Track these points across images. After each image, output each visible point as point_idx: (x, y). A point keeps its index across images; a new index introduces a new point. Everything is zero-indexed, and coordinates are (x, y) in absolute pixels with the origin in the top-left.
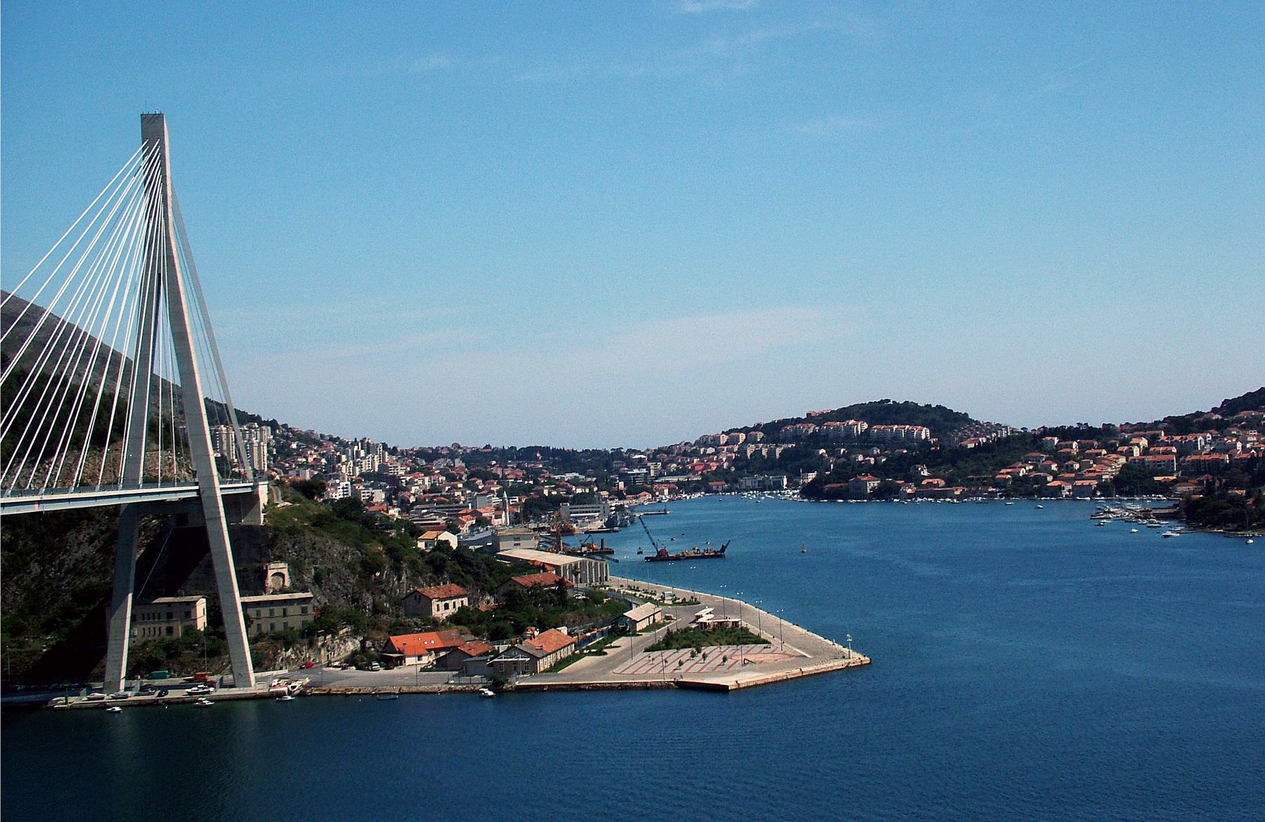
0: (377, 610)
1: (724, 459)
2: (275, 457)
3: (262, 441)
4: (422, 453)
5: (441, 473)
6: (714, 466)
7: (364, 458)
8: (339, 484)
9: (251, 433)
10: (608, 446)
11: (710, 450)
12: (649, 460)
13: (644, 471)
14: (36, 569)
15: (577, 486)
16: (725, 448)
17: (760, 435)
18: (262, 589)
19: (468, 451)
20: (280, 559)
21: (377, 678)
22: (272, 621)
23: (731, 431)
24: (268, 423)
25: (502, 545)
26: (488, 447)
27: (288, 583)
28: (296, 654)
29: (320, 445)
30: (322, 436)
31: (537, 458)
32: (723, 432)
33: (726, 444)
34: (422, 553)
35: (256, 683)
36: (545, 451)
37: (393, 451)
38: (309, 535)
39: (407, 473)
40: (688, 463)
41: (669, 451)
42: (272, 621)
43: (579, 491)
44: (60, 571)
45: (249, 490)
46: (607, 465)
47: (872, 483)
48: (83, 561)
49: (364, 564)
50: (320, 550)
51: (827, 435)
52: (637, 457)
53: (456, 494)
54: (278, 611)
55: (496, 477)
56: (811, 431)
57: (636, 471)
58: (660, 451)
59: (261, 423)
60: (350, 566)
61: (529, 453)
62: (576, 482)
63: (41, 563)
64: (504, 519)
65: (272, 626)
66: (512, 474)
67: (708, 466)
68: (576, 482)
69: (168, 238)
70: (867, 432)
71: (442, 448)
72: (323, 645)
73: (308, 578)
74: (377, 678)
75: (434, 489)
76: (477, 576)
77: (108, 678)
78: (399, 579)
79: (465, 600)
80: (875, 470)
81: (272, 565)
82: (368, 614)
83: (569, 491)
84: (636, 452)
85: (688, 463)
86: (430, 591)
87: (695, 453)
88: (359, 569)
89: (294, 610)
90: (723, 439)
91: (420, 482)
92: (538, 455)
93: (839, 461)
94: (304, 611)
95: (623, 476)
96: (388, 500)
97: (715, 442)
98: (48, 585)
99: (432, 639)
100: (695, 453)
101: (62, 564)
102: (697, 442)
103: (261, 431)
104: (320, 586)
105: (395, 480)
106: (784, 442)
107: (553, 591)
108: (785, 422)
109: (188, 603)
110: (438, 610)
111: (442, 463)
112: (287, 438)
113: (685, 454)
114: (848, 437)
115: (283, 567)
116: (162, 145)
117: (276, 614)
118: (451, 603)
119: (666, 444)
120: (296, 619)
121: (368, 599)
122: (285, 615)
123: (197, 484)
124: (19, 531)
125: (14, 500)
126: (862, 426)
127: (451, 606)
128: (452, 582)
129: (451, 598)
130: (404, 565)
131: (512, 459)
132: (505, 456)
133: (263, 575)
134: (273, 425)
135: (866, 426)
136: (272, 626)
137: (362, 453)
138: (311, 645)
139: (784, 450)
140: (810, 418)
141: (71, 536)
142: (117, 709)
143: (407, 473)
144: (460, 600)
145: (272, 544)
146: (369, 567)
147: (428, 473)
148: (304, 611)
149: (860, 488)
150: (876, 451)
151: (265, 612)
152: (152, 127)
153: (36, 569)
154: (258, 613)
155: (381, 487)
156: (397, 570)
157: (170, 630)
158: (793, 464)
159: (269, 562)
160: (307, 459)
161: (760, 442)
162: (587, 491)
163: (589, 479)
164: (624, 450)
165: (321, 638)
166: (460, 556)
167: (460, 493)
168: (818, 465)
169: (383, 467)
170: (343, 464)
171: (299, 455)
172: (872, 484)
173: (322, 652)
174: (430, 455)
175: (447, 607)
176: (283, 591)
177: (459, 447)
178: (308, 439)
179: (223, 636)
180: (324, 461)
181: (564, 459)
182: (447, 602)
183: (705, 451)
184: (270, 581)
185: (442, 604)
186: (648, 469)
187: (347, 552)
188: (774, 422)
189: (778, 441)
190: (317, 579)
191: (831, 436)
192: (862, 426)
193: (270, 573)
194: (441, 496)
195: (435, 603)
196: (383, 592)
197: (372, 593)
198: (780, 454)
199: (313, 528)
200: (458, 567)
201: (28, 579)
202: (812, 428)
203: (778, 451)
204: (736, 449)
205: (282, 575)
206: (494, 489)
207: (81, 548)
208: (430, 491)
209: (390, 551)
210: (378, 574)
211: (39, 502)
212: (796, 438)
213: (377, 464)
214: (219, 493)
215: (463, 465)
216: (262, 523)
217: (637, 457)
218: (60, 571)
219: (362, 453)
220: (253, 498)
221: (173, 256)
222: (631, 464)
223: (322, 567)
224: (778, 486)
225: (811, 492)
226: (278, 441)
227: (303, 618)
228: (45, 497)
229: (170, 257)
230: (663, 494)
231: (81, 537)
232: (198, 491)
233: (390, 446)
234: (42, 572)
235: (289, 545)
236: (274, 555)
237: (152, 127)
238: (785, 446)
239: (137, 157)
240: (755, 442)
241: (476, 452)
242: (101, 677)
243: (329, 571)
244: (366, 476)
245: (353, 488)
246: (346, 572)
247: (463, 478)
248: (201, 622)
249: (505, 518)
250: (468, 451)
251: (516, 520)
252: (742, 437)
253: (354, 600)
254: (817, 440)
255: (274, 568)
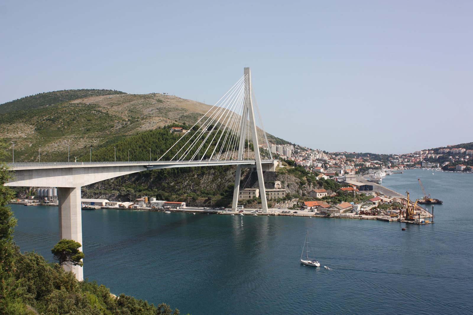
0: (304, 195)
1: (421, 158)
2: (293, 154)
3: (289, 150)
4: (334, 154)
5: (339, 159)
6: (418, 160)
7: (317, 155)
8: (309, 162)
9: (287, 147)
10: (388, 153)
11: (418, 156)
12: (399, 158)
13: (398, 161)
14: (220, 180)
15: (376, 164)
16: (422, 155)
17: (432, 152)
18: (273, 187)
19: (349, 154)
20: (279, 180)
21: (300, 213)
22: (275, 196)
23: (424, 150)
24: (293, 145)
25: (347, 179)
26: (354, 153)
27: (280, 187)
28: (280, 204)
29: (307, 151)
30: (308, 148)
31: (368, 156)
32: (422, 151)
33: (423, 154)
34: (317, 181)
35: (269, 211)
36: (370, 154)
37: (327, 153)
38: (287, 175)
39: (329, 159)
40: (411, 159)
41: (405, 156)
42: (275, 196)
43: (377, 166)
44: (225, 181)
45: (272, 162)
46: (387, 159)
47: (463, 167)
48: (231, 178)
49: (300, 182)
50: (289, 179)
51: (453, 153)
52: (396, 157)
53: (342, 165)
54: (276, 193)
55: (353, 161)
56: (448, 151)
57: (395, 161)
58: (403, 155)
59: (290, 144)
60: (297, 183)
61: (365, 155)
62: (377, 163)
63: (221, 179)
64: (353, 173)
65: (275, 197)
66: (359, 161)
67: (416, 160)
68: (377, 163)
69: (250, 98)
70: (465, 152)
71: (342, 153)
72: (287, 203)
73: (286, 185)
74: (300, 213)
75: (336, 164)
76: (331, 188)
77: (233, 207)
78: (310, 187)
79: (326, 193)
80: (464, 163)
81: (276, 182)
82: (301, 195)
83: (374, 166)
84: (396, 155)
85: (411, 159)
86: (316, 190)
87: (413, 156)
88: (299, 184)
89: (280, 193)
90: (422, 152)
91: (332, 162)
92: (368, 155)
93: (456, 160)
94: (283, 194)
95: (391, 162)
96: (322, 166)
97: (419, 154)
98: (222, 184)
99: (316, 203)
100: (413, 156)
101: (226, 179)
102: (414, 153)
103: (290, 146)
104: (289, 188)
105: (325, 161)
106: (440, 154)
107: (351, 192)
108: (440, 148)
109: (254, 190)
110: (318, 195)
111: (339, 157)
112: (298, 149)
113: (410, 156)
114: (459, 154)
115: (279, 182)
116: (249, 75)
117: (276, 194)
118: (322, 194)
119: (405, 153)
120: (281, 197)
121: (301, 192)
122: (278, 194)
123: (255, 160)
124: (216, 170)
125: (201, 163)
126: (463, 150)
127: (322, 195)
128: (324, 189)
129: (322, 193)
130: (312, 183)
131: (361, 156)
132: (358, 155)
133: (274, 184)
134: (294, 145)
135: (465, 150)
136: (275, 197)
137: (317, 153)
138: (284, 202)
139: (440, 156)
140: (448, 147)
141: (228, 172)
142: (234, 215)
143: (329, 159)
144: (325, 193)
145: (276, 176)
146: (302, 184)
147: (334, 159)
148: (283, 194)
149: (459, 168)
150: (468, 157)
151: (273, 193)
152: (246, 71)
153: (220, 180)
154: (271, 193)
155: (321, 163)
156: (309, 185)
157: (250, 197)
158: (441, 160)
159: (276, 181)
160: (302, 154)
161: (432, 154)
162: (379, 166)
163: (381, 163)
164: (393, 155)
165: (287, 201)
166: (326, 182)
167: (343, 165)
168: (450, 160)
169: (322, 157)
170: (311, 156)
171: (300, 153)
172: (463, 167)
173: (287, 205)
174: (336, 155)
175: (321, 195)
176: (279, 188)
177: (346, 152)
178: (303, 149)
179: (261, 198)
180: (306, 155)
181: (375, 157)
182: (321, 193)
183: (416, 156)
184: (276, 186)
185: (320, 194)
186: (399, 160)
187: (296, 179)
188: (437, 148)
189: (437, 154)
190: (288, 186)
191: (454, 153)
192: (463, 150)
193: (276, 184)
194: (337, 166)
195: (318, 194)
196: (305, 190)
197: (302, 190)
198: (438, 157)
199: (288, 173)
200: (326, 185)
201: (218, 182)
202: (448, 150)
203: (438, 156)
204: (425, 155)
205: (279, 184)
206: (352, 164)
207: (230, 174)
208: (334, 164)
209: (308, 180)
210: (304, 185)
211: (208, 163)
212: (443, 153)
213: (321, 156)
214: (261, 163)
215: (345, 157)
216: (275, 171)
217: (396, 157)
218: (225, 181)
219: (317, 153)
220: (272, 165)
221: (251, 103)
222: (394, 159)
223: (289, 183)
224: (437, 167)
225: (445, 169)
226: (295, 150)
227: (283, 196)
228: (210, 163)
229: (250, 103)
230: (401, 167)
231: (230, 173)
232: (255, 162)
233: (326, 152)
234: (221, 180)
235: (281, 177)
236: (277, 179)
237: (246, 71)
238: (440, 155)
239: (243, 78)
240: (431, 154)
241: (351, 154)
242: (231, 207)
243: (291, 184)
244: (318, 160)
245: (313, 163)
246: (296, 184)
247: (345, 161)
248: (257, 196)
249: (353, 172)
250: (349, 154)
251: (357, 173)
252: (427, 152)
253: (298, 192)
254: (449, 153)
255: (277, 183)
